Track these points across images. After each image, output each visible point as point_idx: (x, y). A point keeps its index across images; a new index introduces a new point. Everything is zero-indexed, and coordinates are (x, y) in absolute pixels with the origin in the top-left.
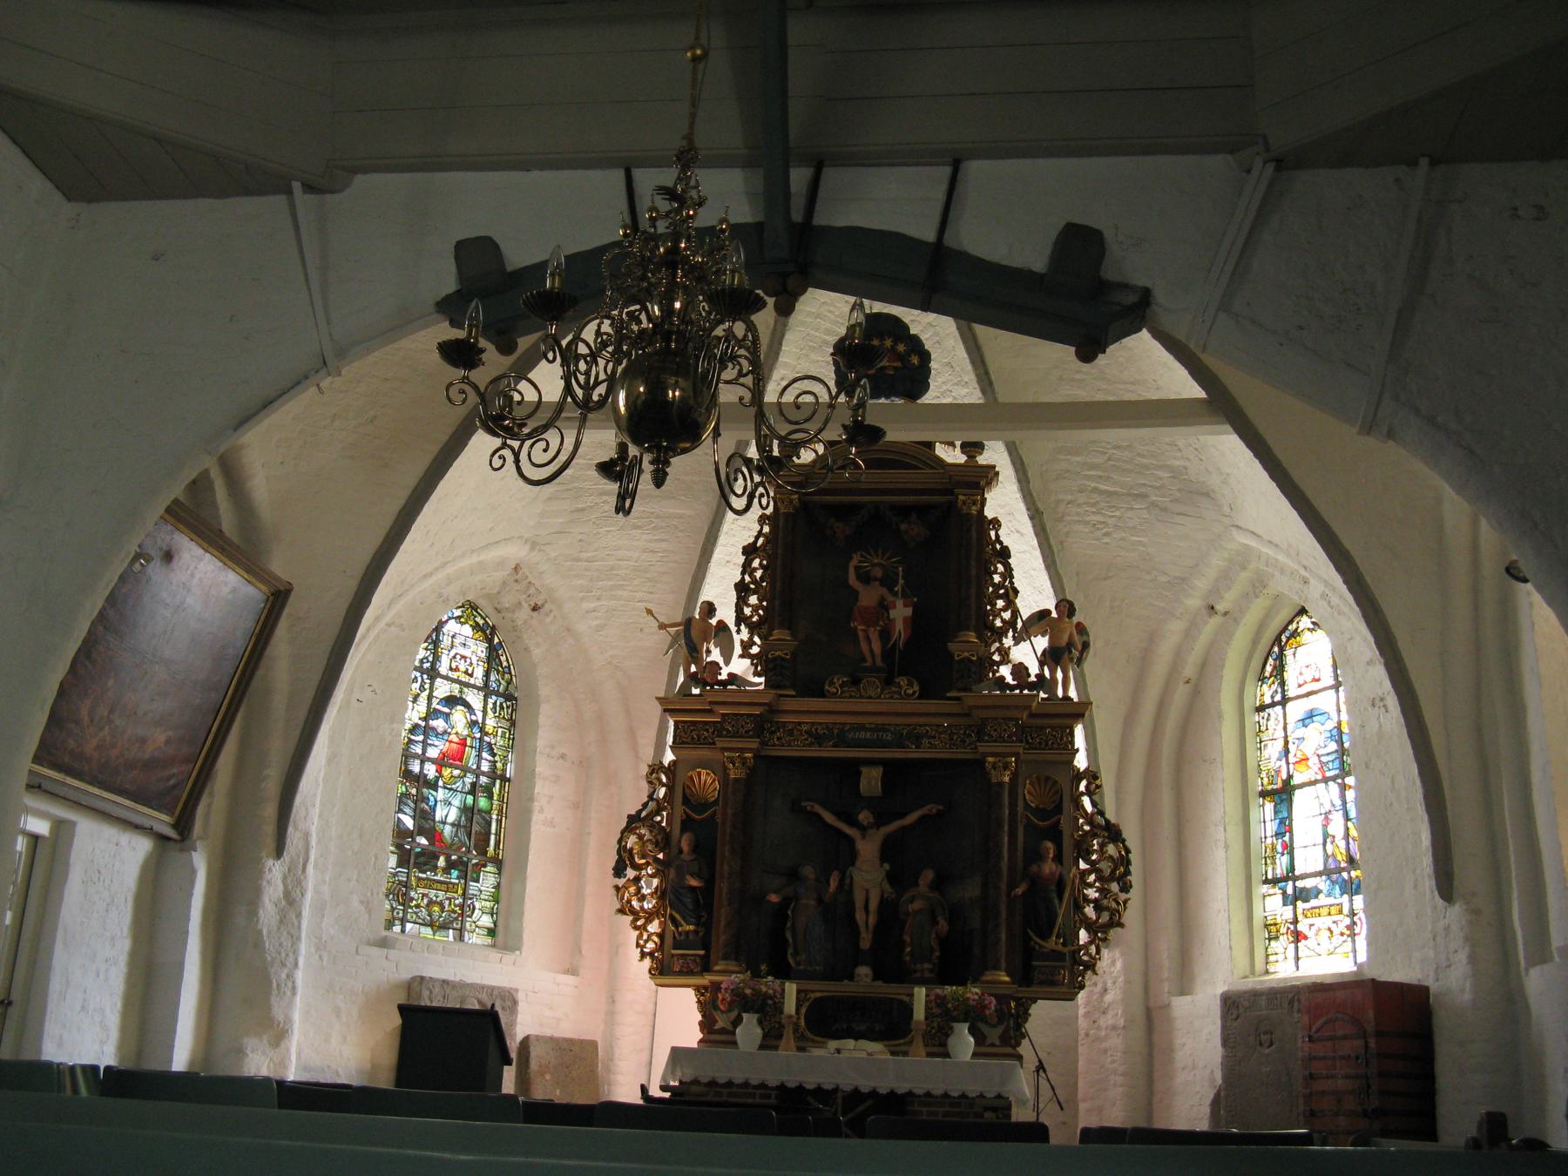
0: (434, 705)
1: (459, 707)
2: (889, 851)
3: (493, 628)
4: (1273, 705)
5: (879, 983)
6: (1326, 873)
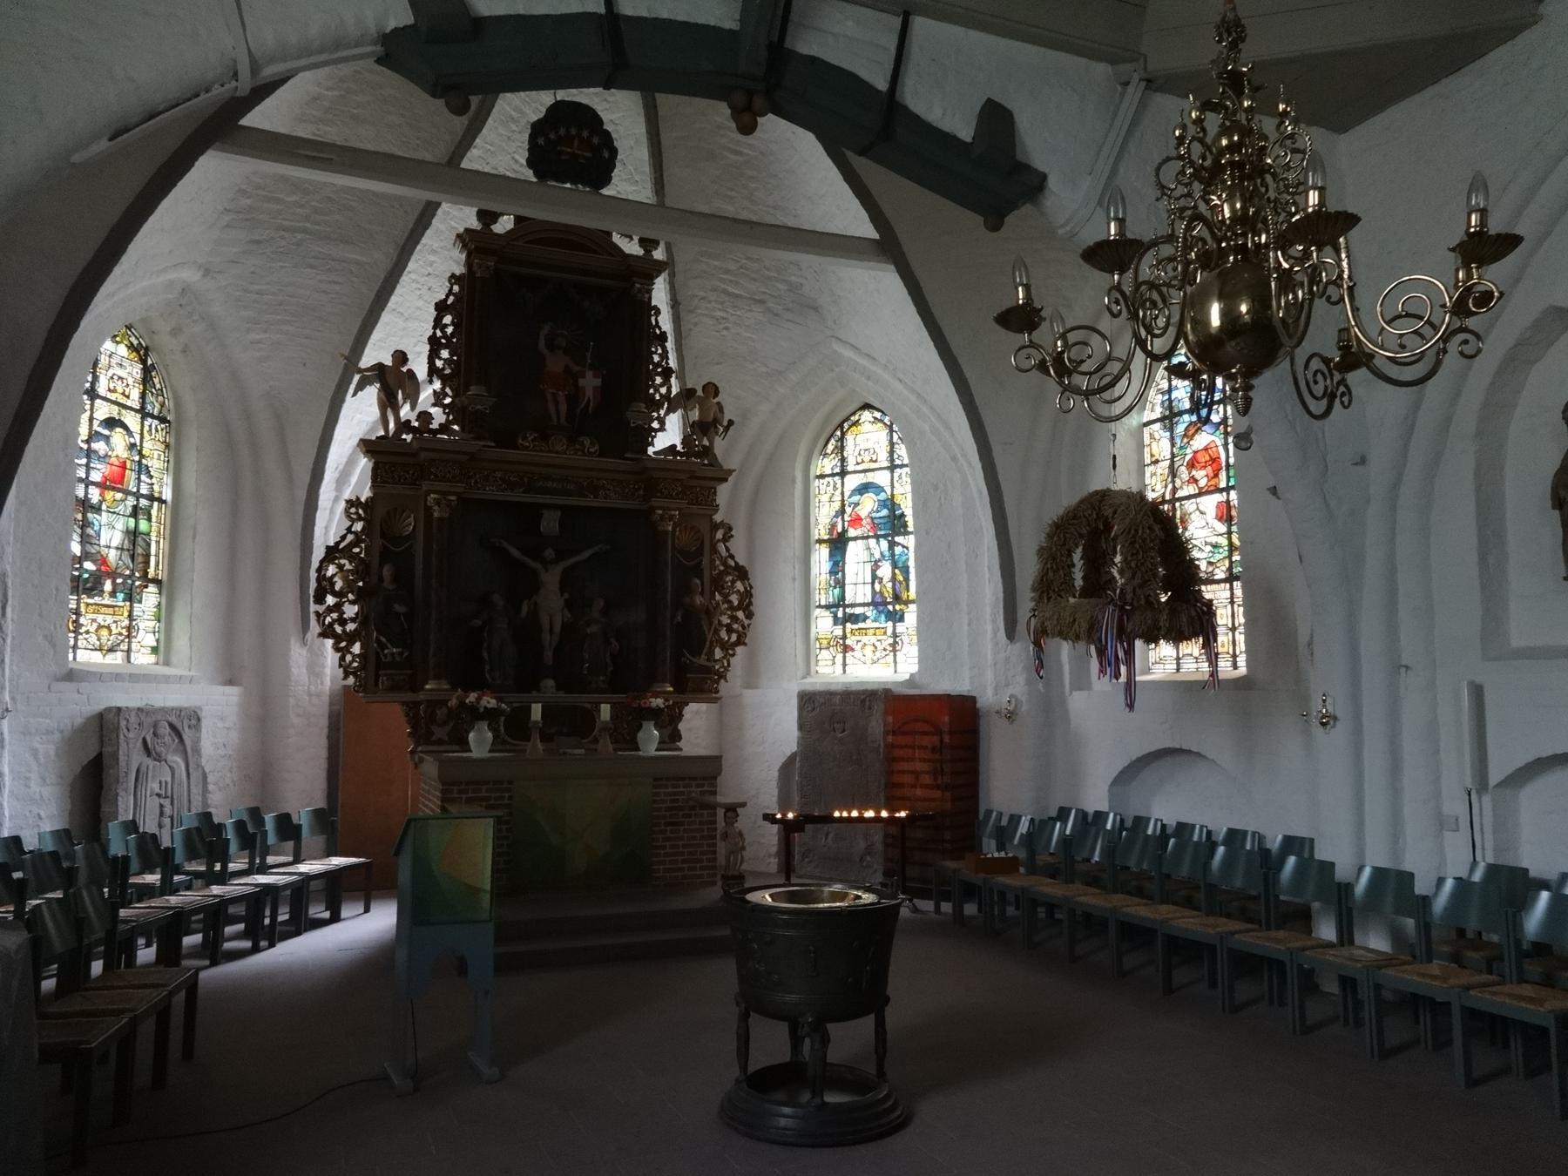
0: (96, 427)
1: (118, 430)
3: (147, 349)
4: (833, 475)
5: (561, 694)
6: (874, 604)
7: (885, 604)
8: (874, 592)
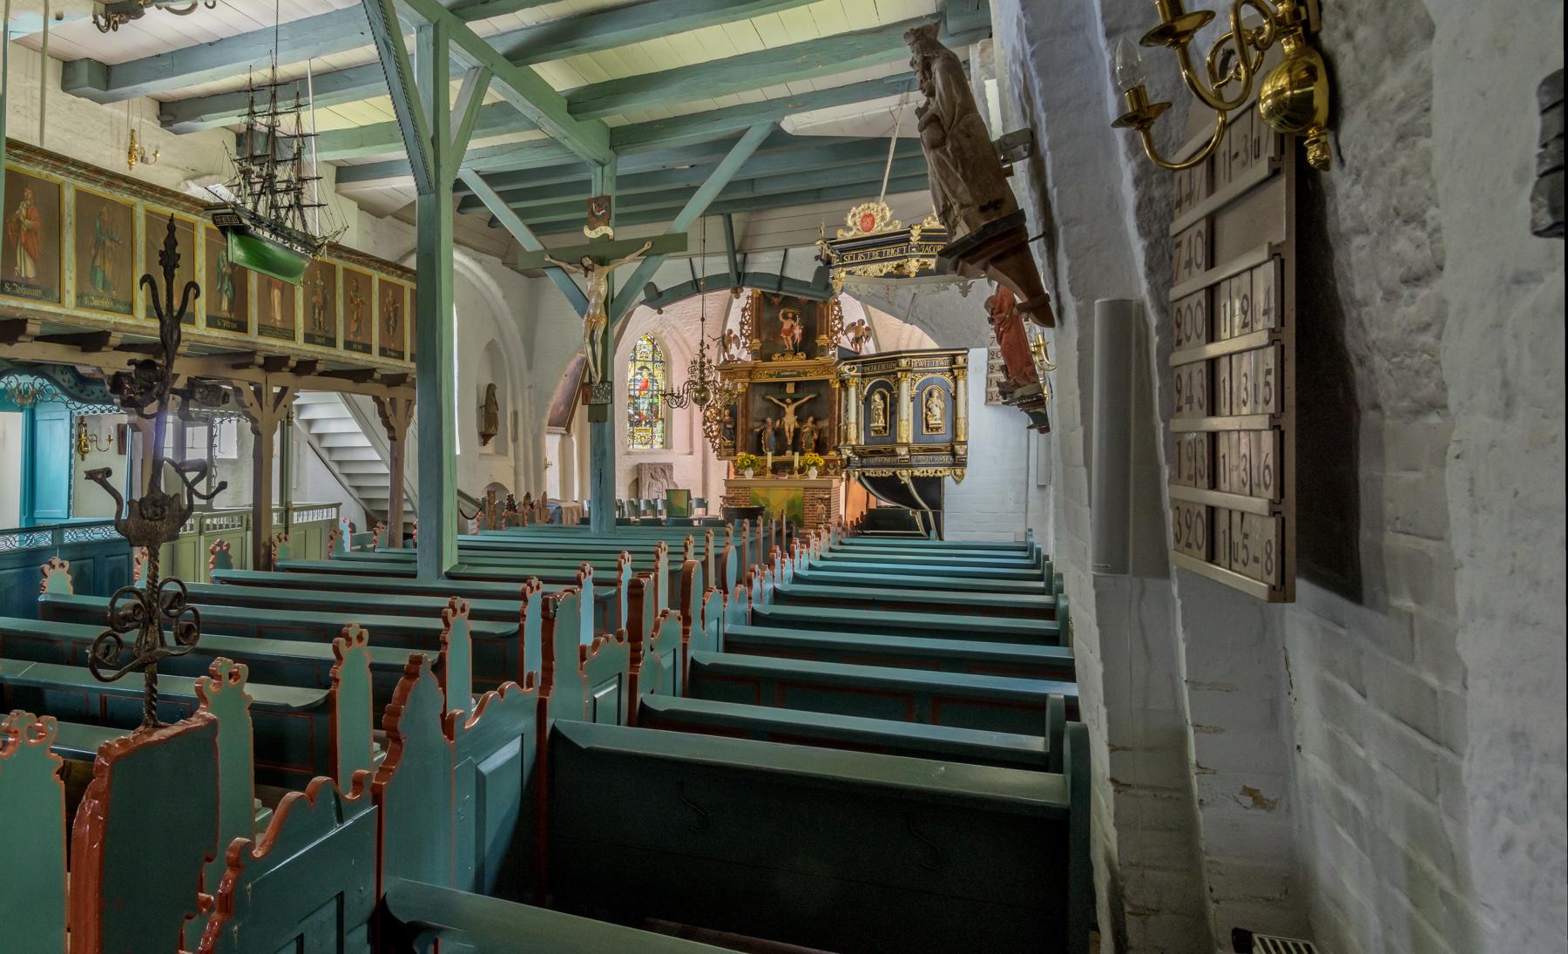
2: (797, 411)
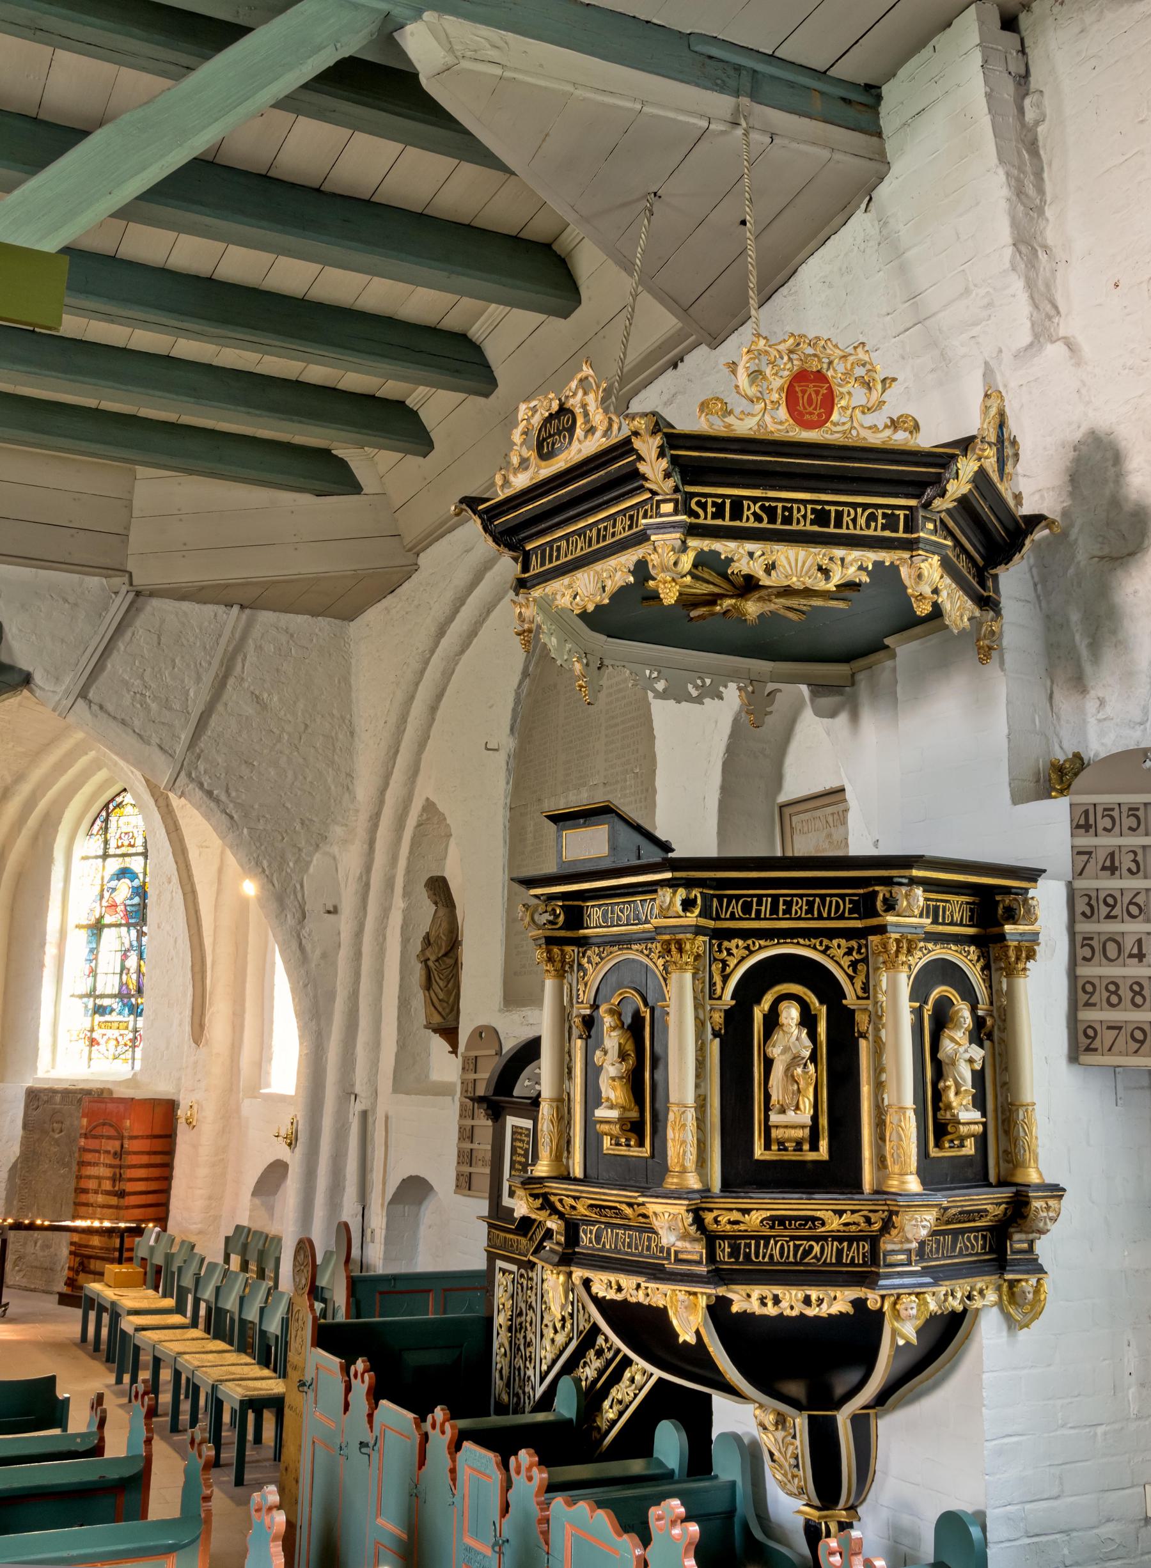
6: (120, 995)
7: (129, 996)
8: (121, 985)
